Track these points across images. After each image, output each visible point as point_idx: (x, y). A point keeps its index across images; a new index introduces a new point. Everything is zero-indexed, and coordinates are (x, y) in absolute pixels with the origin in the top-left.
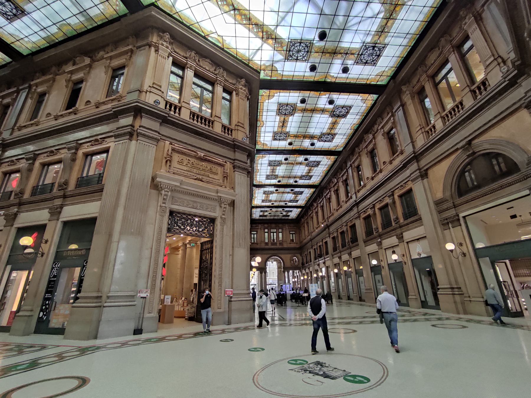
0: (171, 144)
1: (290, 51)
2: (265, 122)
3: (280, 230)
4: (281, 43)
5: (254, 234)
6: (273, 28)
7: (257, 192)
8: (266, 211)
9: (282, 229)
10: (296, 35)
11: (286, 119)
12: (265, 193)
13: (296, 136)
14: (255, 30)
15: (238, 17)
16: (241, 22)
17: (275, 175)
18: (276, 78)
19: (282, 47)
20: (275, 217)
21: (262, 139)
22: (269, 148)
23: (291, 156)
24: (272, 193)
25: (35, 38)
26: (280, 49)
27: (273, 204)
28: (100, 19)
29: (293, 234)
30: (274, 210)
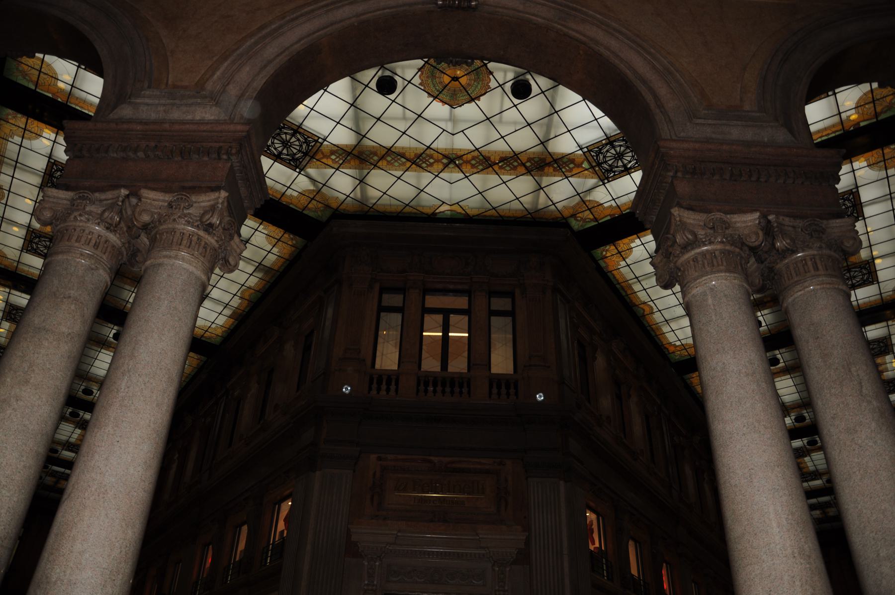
0: (379, 459)
1: (599, 164)
2: (651, 303)
4: (572, 161)
6: (540, 148)
10: (590, 136)
14: (508, 168)
15: (467, 168)
16: (475, 170)
18: (609, 218)
19: (579, 165)
21: (671, 337)
23: (783, 350)
25: (222, 320)
26: (575, 171)
28: (279, 264)
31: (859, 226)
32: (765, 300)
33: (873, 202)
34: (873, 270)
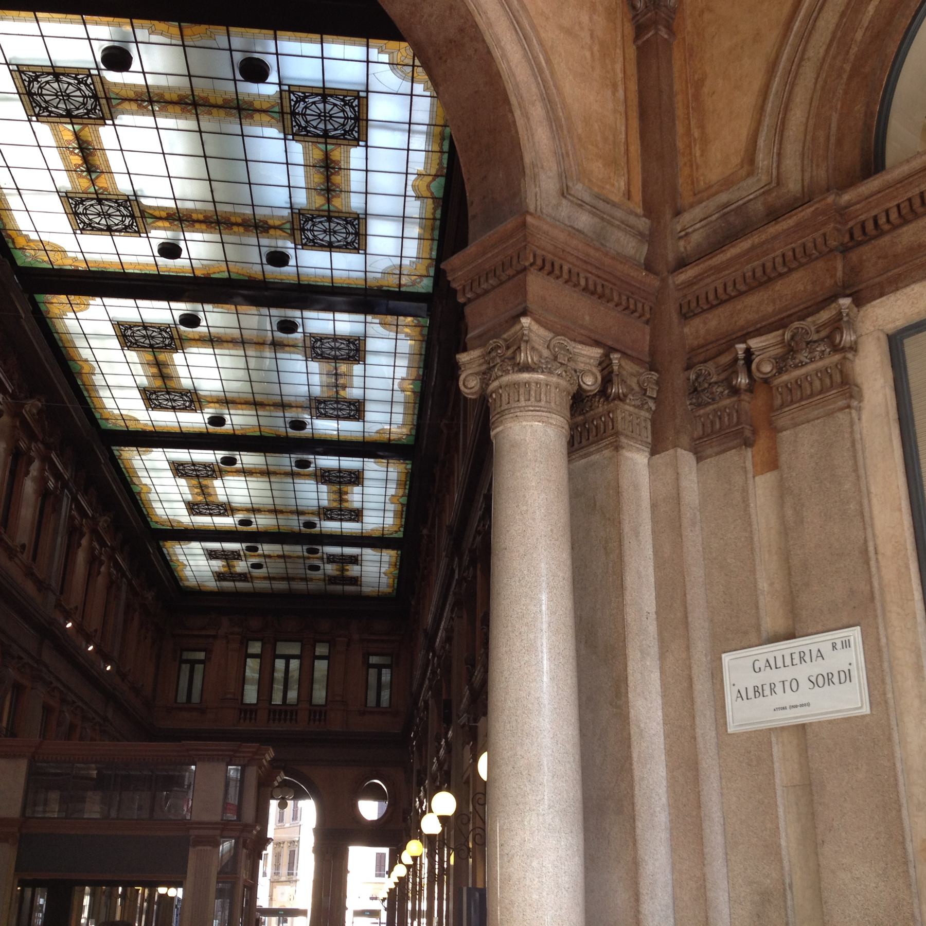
3: (322, 650)
5: (193, 663)
7: (137, 463)
8: (236, 555)
9: (332, 644)
11: (87, 133)
12: (178, 469)
13: (179, 218)
17: (184, 393)
20: (300, 586)
22: (82, 266)
23: (208, 307)
24: (212, 471)
27: (245, 522)
29: (379, 667)
30: (266, 548)
31: (356, 155)
32: (195, 216)
33: (387, 125)
34: (362, 232)
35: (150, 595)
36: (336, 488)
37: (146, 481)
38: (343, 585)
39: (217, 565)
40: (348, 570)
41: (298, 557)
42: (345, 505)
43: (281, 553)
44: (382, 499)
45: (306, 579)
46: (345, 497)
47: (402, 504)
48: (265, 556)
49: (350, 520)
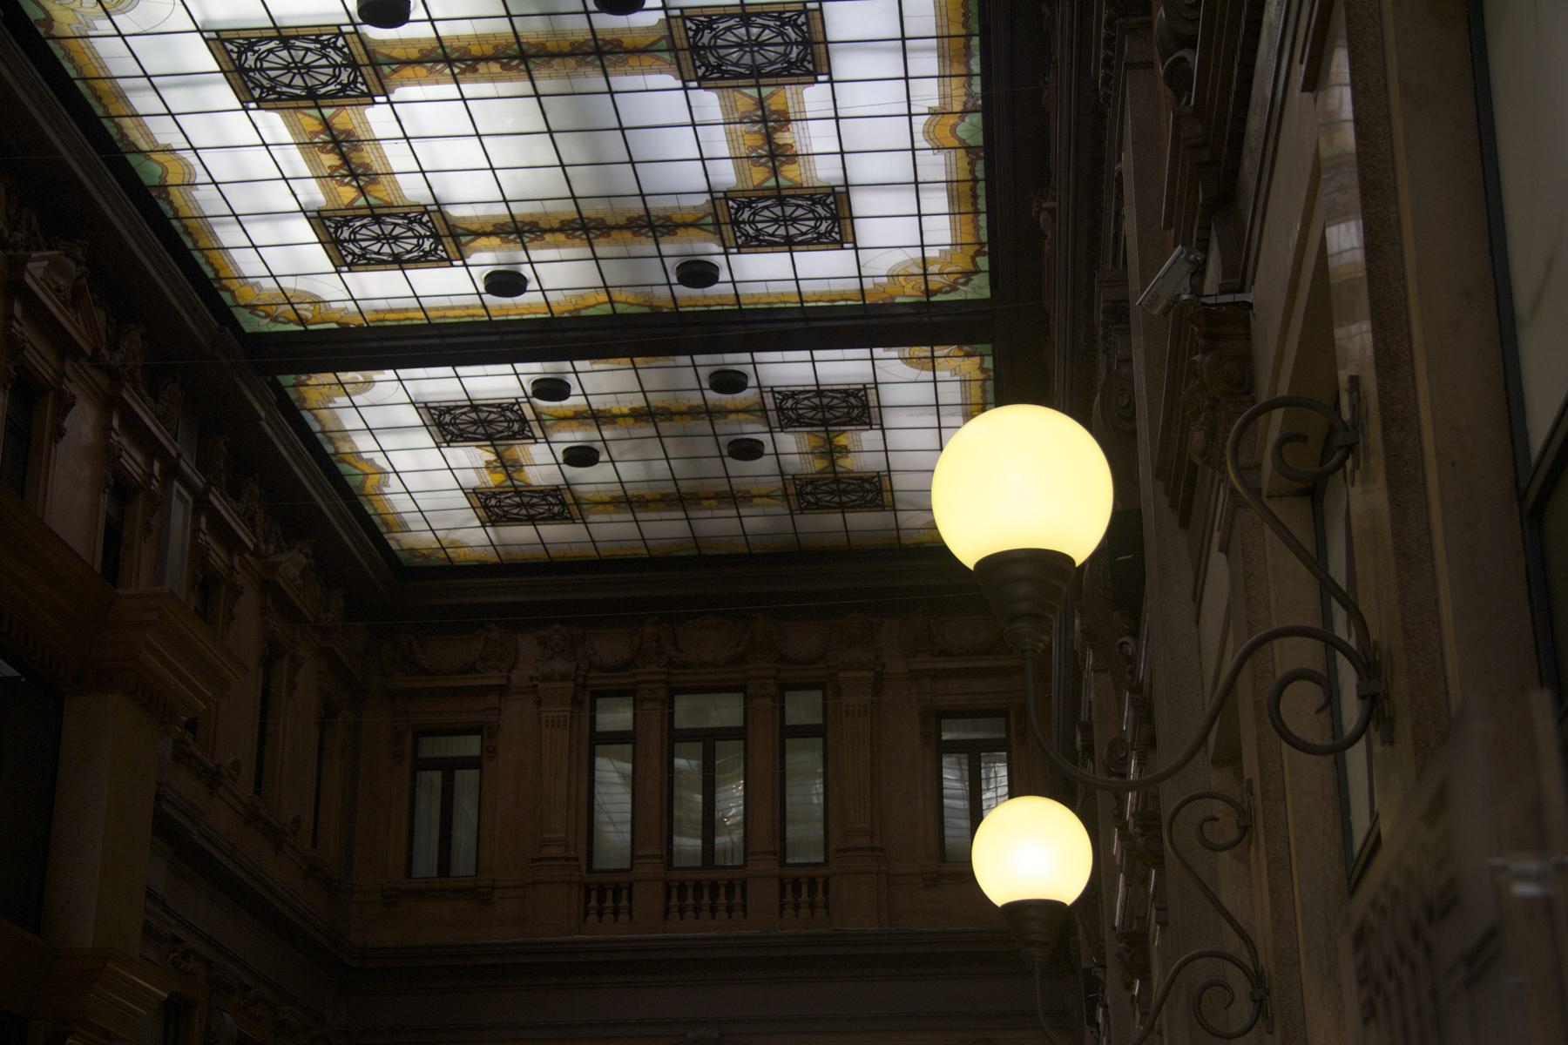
3: (802, 708)
5: (449, 767)
20: (718, 524)
27: (505, 282)
35: (292, 563)
36: (745, 98)
37: (164, 132)
38: (842, 508)
39: (471, 460)
40: (845, 450)
41: (693, 412)
42: (791, 173)
43: (638, 401)
44: (897, 132)
45: (734, 498)
46: (782, 138)
47: (968, 149)
48: (596, 417)
49: (819, 241)
